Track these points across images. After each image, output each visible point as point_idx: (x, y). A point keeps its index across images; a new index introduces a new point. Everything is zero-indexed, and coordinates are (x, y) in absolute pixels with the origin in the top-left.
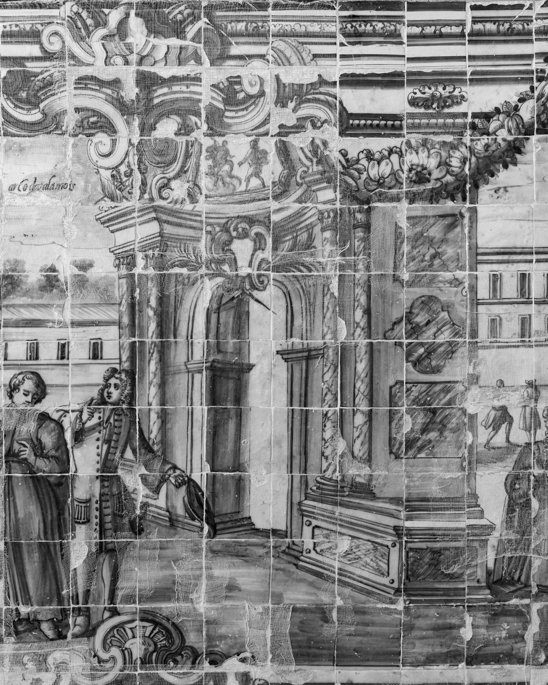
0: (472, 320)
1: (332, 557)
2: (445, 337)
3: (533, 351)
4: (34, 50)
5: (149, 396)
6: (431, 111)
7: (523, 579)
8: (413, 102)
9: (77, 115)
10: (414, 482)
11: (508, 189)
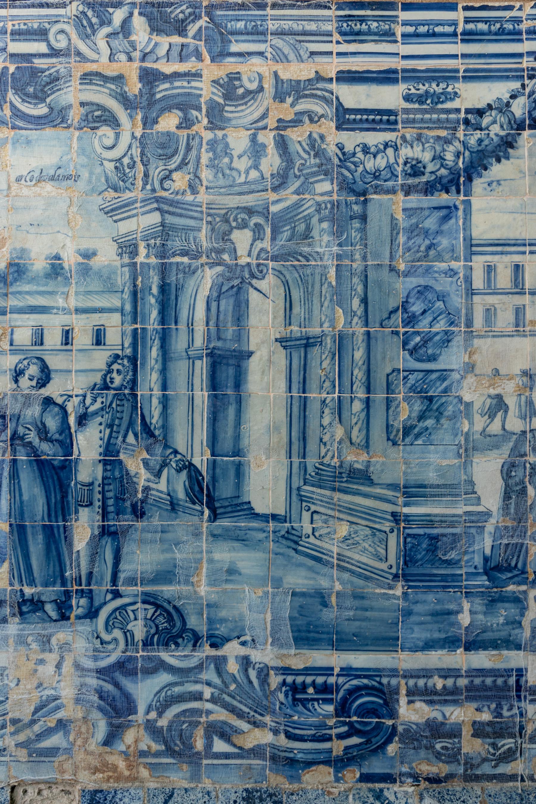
0: (467, 309)
1: (331, 542)
2: (440, 326)
3: (527, 341)
4: (42, 48)
5: (150, 382)
6: (425, 107)
7: (520, 565)
8: (407, 98)
9: (82, 109)
10: (411, 468)
11: (502, 182)
